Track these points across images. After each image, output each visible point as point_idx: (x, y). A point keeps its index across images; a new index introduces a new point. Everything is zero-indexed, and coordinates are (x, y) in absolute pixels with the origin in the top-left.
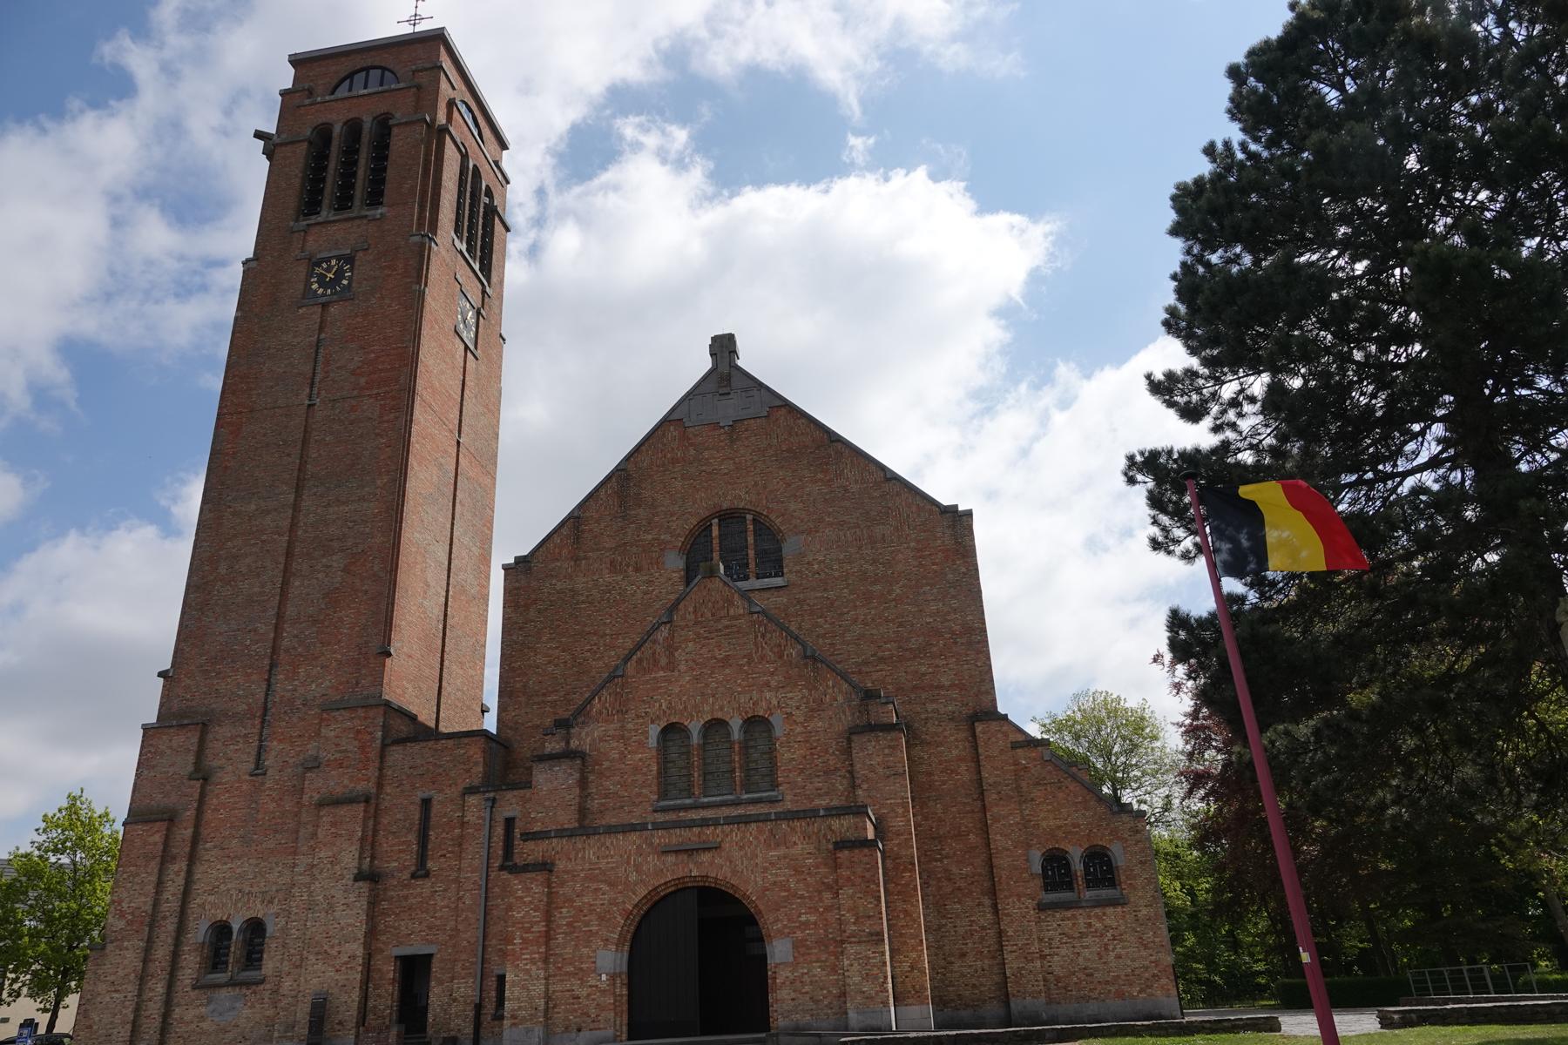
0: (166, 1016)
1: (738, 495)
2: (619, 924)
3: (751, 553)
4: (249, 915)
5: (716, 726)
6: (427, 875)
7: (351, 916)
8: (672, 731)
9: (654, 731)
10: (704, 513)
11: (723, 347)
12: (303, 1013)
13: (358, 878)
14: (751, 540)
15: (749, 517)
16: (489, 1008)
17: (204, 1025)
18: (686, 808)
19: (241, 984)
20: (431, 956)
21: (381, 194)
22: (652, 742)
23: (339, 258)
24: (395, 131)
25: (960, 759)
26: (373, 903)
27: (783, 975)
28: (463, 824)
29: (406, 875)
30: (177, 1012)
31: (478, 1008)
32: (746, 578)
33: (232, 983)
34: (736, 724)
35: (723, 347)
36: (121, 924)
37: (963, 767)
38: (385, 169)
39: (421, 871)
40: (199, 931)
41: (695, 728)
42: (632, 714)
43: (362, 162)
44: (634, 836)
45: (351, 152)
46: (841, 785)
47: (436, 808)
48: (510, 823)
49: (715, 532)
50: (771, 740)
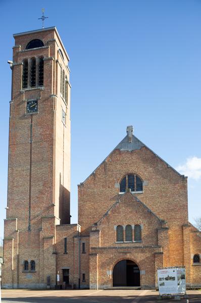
0: (18, 277)
1: (133, 169)
2: (112, 267)
3: (135, 184)
5: (129, 226)
6: (67, 253)
7: (52, 260)
8: (119, 227)
9: (115, 227)
10: (124, 174)
11: (129, 129)
12: (45, 278)
13: (53, 253)
14: (135, 181)
15: (135, 175)
16: (82, 279)
17: (26, 279)
18: (122, 243)
19: (32, 272)
20: (68, 270)
21: (43, 82)
24: (45, 62)
25: (179, 235)
26: (57, 259)
28: (74, 244)
29: (62, 253)
30: (20, 277)
31: (79, 279)
32: (134, 190)
33: (30, 272)
35: (129, 129)
36: (7, 260)
37: (179, 236)
38: (43, 74)
39: (66, 253)
40: (22, 262)
42: (110, 223)
43: (37, 72)
44: (114, 249)
45: (33, 72)
46: (155, 240)
47: (68, 240)
48: (84, 244)
49: (127, 178)
50: (140, 230)
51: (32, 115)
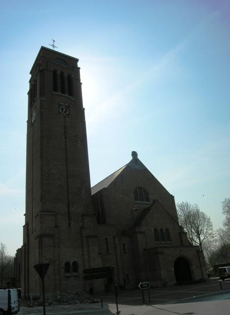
4: (74, 261)
5: (161, 229)
8: (156, 230)
9: (153, 229)
11: (134, 154)
22: (153, 231)
23: (65, 106)
27: (195, 271)
31: (125, 280)
34: (164, 229)
35: (134, 154)
40: (63, 265)
41: (159, 229)
51: (65, 117)
